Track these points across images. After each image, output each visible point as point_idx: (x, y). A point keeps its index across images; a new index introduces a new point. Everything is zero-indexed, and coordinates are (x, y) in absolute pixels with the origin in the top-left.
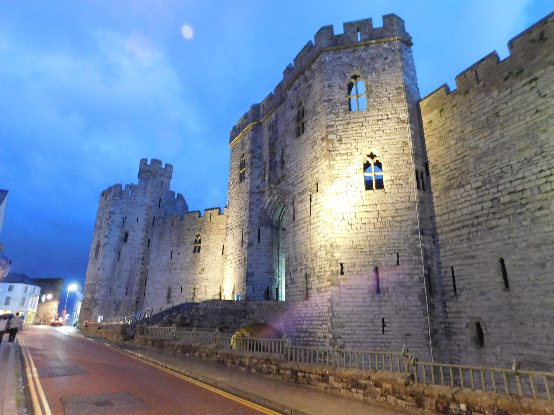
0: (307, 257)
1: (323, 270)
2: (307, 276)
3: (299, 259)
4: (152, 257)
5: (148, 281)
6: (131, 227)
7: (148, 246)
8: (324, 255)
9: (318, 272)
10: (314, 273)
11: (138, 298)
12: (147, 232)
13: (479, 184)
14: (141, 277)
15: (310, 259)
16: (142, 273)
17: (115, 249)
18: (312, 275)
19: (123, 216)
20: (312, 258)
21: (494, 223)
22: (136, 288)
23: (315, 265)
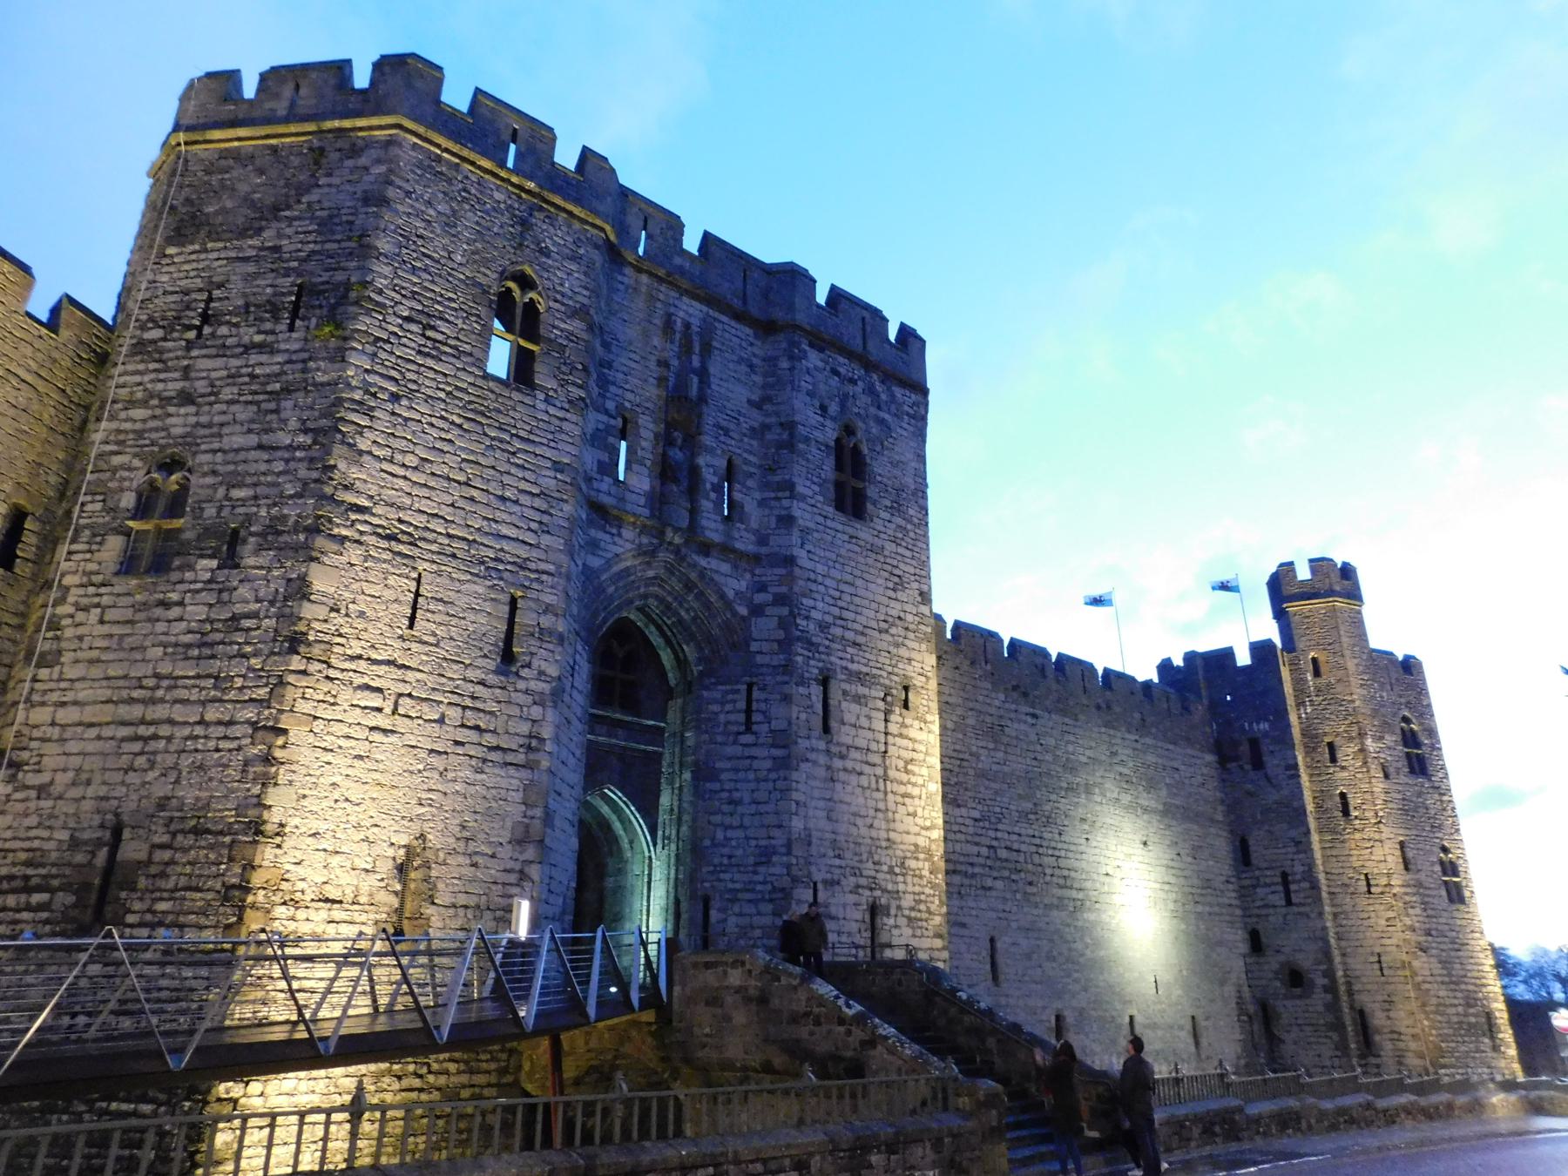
0: (876, 858)
1: (922, 907)
2: (874, 910)
3: (848, 855)
8: (926, 873)
9: (912, 909)
10: (899, 908)
13: (976, 814)
15: (885, 868)
18: (893, 912)
20: (891, 867)
21: (989, 882)
23: (901, 887)
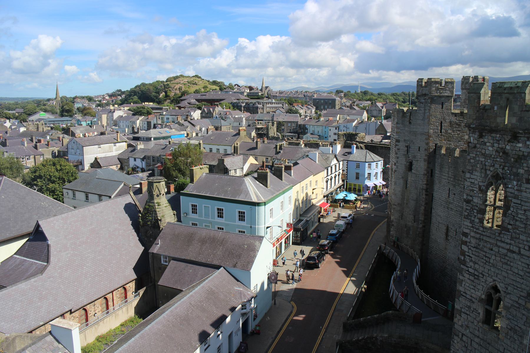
4: (436, 187)
5: (433, 211)
6: (414, 157)
7: (432, 176)
11: (424, 226)
12: (429, 163)
14: (425, 208)
16: (426, 204)
17: (403, 178)
19: (407, 145)
22: (422, 218)
